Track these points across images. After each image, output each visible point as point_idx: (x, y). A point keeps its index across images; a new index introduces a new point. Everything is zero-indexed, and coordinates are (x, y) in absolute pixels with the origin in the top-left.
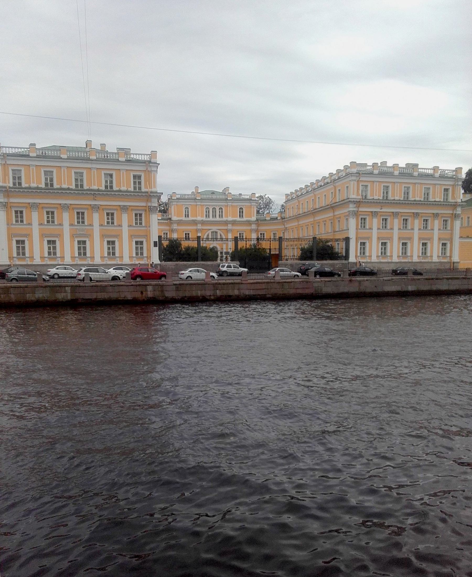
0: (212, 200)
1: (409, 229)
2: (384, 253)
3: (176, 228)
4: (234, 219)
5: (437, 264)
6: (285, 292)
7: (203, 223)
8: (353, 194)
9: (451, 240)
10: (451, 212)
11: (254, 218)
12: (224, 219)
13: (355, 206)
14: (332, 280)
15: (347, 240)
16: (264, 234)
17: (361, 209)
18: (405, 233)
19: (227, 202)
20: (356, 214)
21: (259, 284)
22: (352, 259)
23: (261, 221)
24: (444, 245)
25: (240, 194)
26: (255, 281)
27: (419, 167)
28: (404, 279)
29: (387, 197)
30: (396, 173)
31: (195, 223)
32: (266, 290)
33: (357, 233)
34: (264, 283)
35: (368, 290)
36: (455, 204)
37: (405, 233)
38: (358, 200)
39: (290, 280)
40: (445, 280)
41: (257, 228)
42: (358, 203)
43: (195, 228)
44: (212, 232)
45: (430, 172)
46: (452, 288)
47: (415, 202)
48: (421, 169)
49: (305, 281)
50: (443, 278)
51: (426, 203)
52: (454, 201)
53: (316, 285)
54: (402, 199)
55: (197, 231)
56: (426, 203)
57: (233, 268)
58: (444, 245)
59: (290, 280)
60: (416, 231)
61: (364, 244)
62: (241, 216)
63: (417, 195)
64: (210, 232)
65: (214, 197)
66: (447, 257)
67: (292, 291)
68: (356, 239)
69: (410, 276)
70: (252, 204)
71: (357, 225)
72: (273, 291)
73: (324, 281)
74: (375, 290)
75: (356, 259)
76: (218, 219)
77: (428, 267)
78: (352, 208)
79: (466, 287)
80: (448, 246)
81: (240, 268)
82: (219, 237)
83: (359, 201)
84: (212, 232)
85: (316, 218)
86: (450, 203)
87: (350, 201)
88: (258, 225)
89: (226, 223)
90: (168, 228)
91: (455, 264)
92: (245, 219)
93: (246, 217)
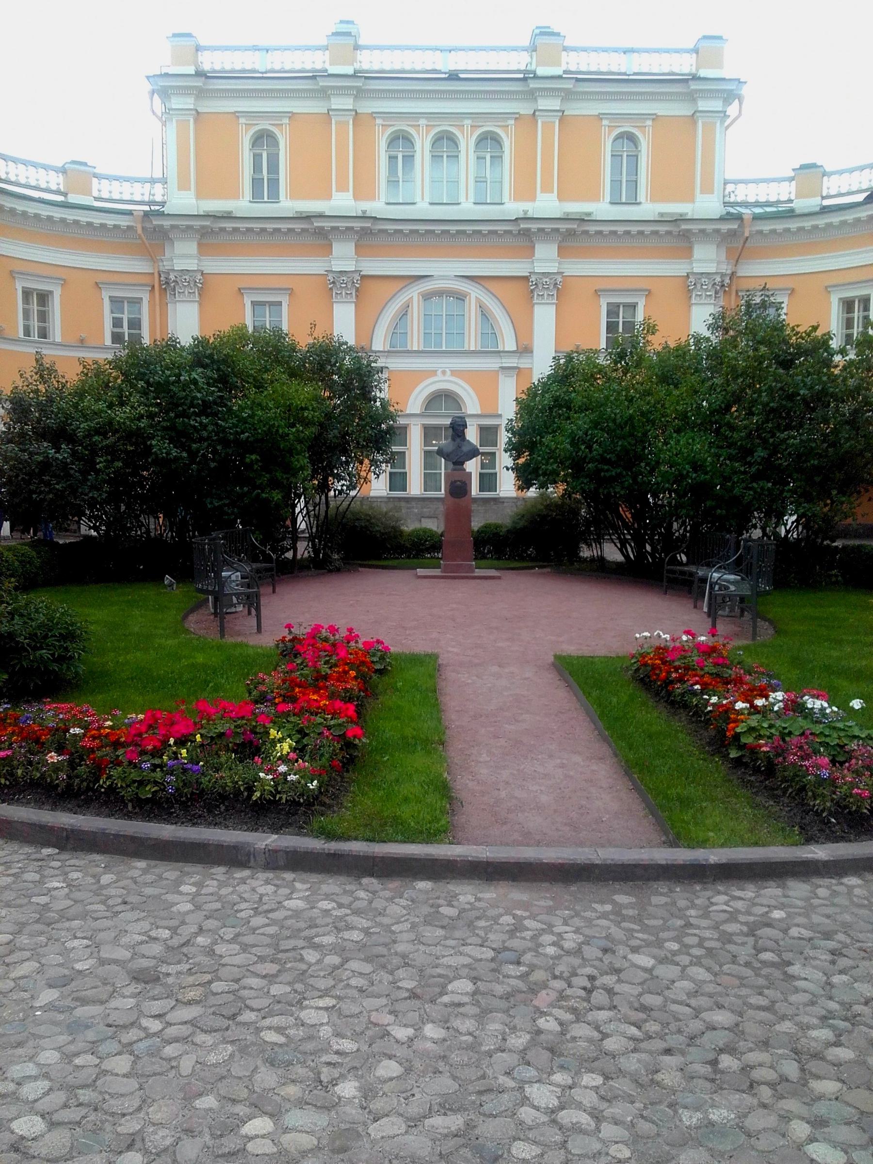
3: (191, 265)
4: (575, 208)
31: (315, 232)
41: (726, 269)
43: (314, 266)
44: (427, 296)
70: (702, 105)
84: (427, 296)
93: (654, 198)
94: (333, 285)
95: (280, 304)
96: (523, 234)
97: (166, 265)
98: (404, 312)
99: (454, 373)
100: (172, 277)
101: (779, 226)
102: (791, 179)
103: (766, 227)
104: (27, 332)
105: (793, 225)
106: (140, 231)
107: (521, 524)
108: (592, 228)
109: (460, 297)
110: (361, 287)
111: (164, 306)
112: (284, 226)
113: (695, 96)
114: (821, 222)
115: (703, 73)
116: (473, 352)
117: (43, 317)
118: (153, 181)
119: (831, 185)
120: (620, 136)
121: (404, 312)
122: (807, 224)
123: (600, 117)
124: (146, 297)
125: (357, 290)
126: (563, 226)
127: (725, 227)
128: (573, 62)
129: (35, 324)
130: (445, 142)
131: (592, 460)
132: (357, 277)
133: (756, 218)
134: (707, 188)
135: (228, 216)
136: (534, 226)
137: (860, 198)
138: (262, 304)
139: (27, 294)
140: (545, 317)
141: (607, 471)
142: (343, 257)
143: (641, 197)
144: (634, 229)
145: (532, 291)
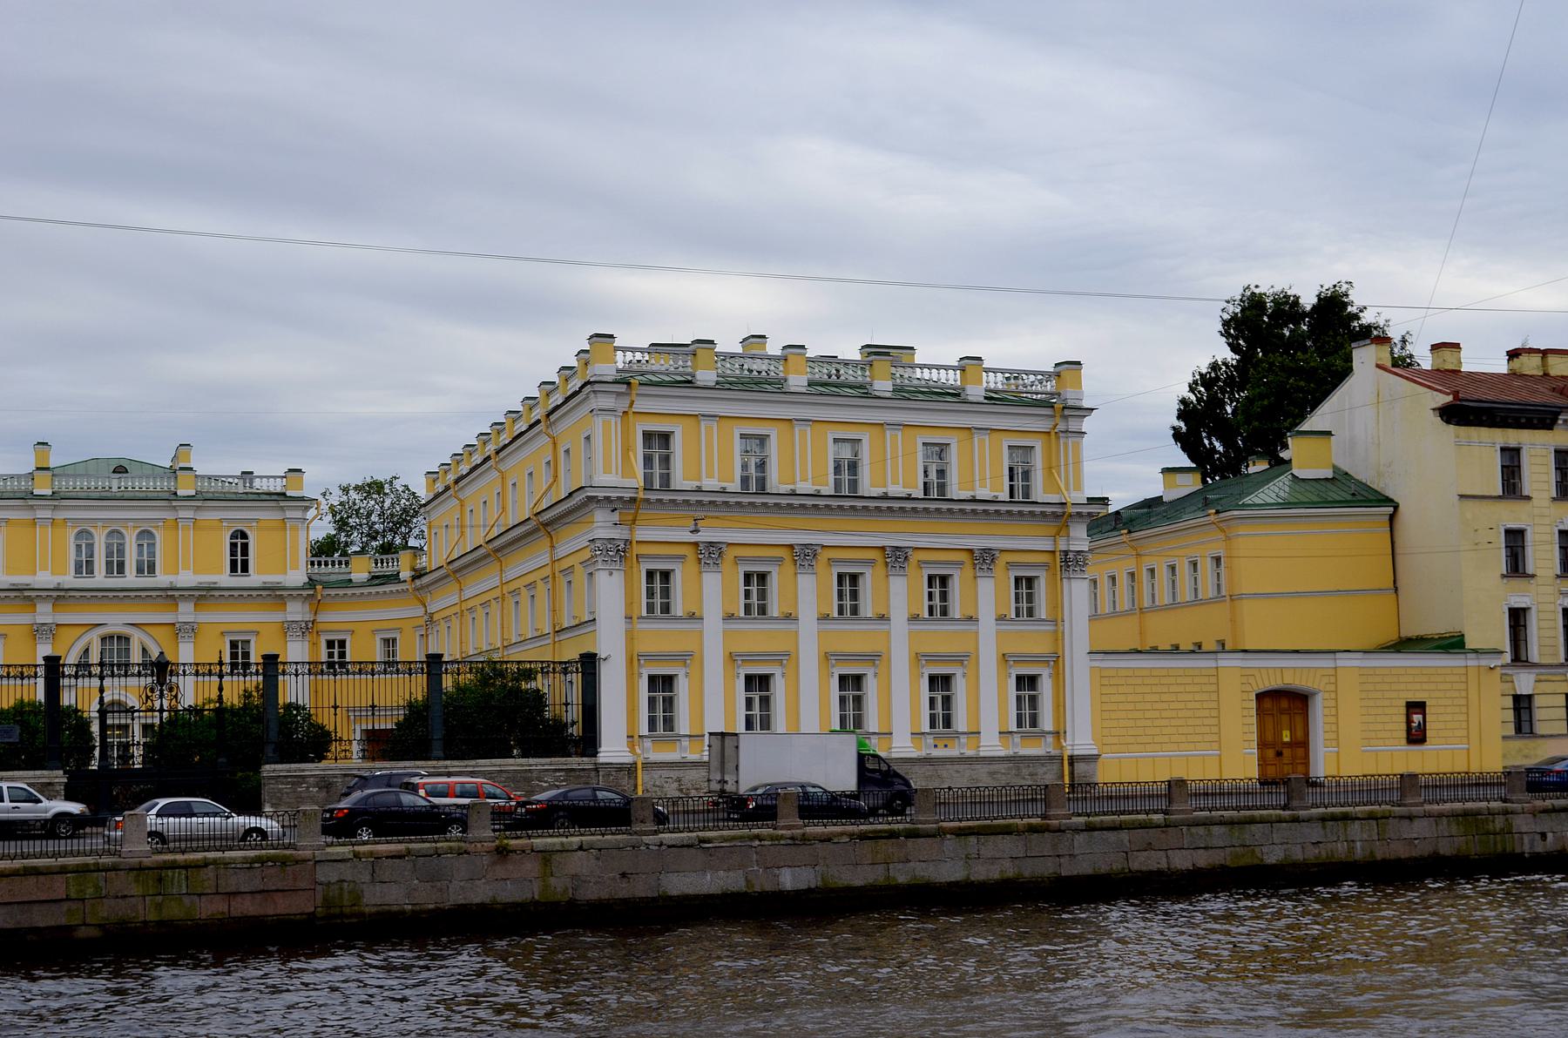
0: (105, 497)
1: (772, 618)
2: (943, 719)
5: (1002, 767)
6: (174, 911)
7: (60, 596)
8: (607, 471)
9: (1055, 660)
10: (1047, 545)
11: (296, 576)
12: (162, 579)
13: (616, 517)
14: (409, 852)
15: (589, 663)
16: (342, 644)
17: (642, 534)
18: (758, 637)
20: (620, 552)
21: (32, 880)
22: (613, 748)
23: (327, 585)
24: (1027, 682)
25: (247, 474)
26: (18, 864)
27: (918, 360)
28: (758, 837)
29: (762, 482)
30: (797, 381)
32: (74, 906)
33: (630, 637)
34: (63, 870)
35: (591, 893)
36: (1059, 510)
37: (852, 637)
38: (627, 495)
39: (200, 856)
40: (950, 843)
42: (627, 506)
43: (25, 619)
45: (952, 379)
46: (983, 872)
47: (884, 504)
48: (922, 367)
49: (269, 859)
50: (940, 833)
51: (847, 503)
52: (1055, 499)
53: (326, 874)
54: (829, 489)
55: (38, 632)
56: (847, 503)
57: (7, 804)
58: (1027, 682)
59: (200, 856)
60: (987, 625)
61: (667, 682)
62: (239, 564)
63: (983, 480)
64: (94, 638)
65: (126, 483)
66: (1044, 734)
67: (208, 908)
68: (630, 661)
69: (790, 823)
70: (289, 514)
71: (629, 604)
72: (107, 911)
73: (371, 854)
74: (624, 891)
75: (632, 750)
76: (131, 579)
77: (959, 779)
78: (602, 525)
79: (1045, 868)
80: (1046, 688)
81: (46, 803)
82: (136, 657)
83: (633, 500)
85: (511, 574)
86: (1038, 509)
87: (590, 499)
88: (317, 605)
89: (170, 596)
91: (1080, 768)
92: (255, 578)
109: (124, 639)
122: (358, 591)
123: (221, 520)
126: (197, 593)
127: (305, 593)
134: (295, 567)
136: (176, 594)
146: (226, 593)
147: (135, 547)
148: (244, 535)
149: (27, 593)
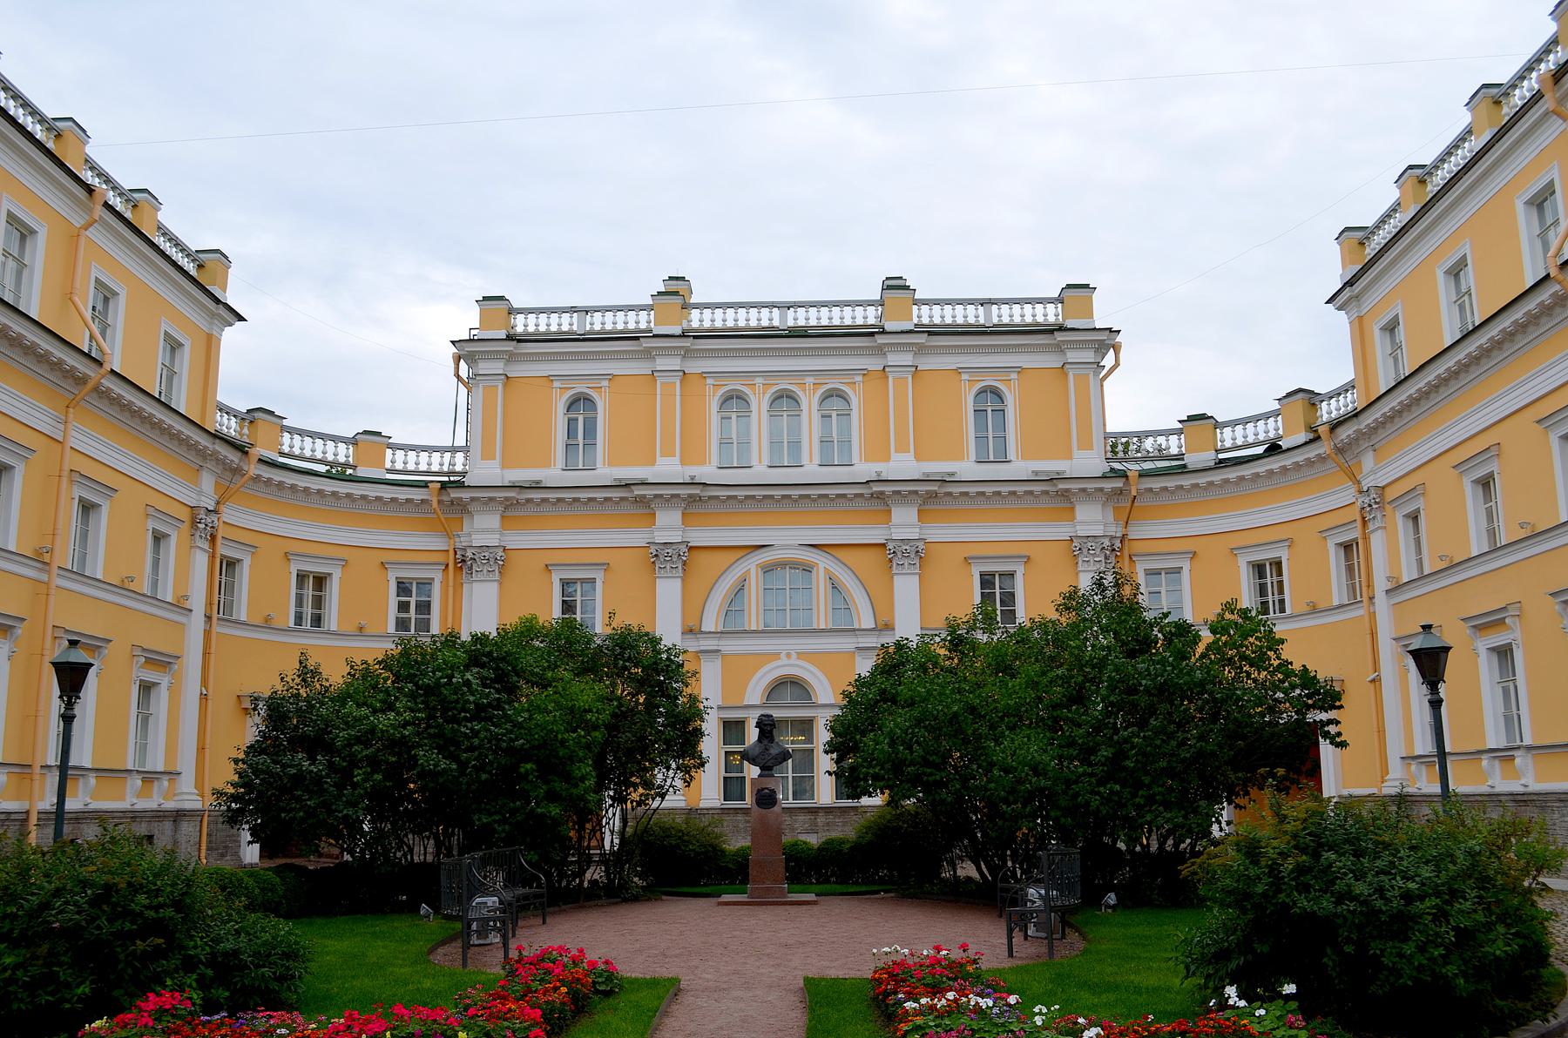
3: (492, 540)
19: (880, 351)
31: (635, 499)
43: (636, 537)
84: (768, 569)
90: (435, 543)
93: (1026, 455)
94: (657, 557)
95: (593, 581)
96: (878, 496)
97: (463, 542)
98: (740, 589)
99: (800, 655)
100: (469, 554)
101: (1171, 482)
102: (1179, 432)
103: (1156, 484)
104: (299, 619)
105: (1186, 481)
106: (435, 504)
107: (869, 837)
108: (956, 489)
109: (807, 569)
110: (685, 558)
111: (458, 587)
112: (600, 495)
113: (1071, 338)
114: (1217, 477)
115: (1070, 324)
116: (823, 631)
117: (318, 602)
118: (454, 450)
119: (1227, 437)
120: (982, 391)
121: (740, 589)
122: (1202, 480)
123: (958, 371)
124: (438, 576)
125: (684, 563)
127: (1108, 485)
128: (925, 315)
129: (308, 610)
130: (785, 398)
131: (912, 763)
132: (683, 548)
133: (1143, 474)
134: (1086, 444)
135: (537, 486)
136: (888, 489)
137: (1260, 450)
138: (574, 581)
139: (302, 577)
140: (906, 588)
141: (931, 774)
142: (669, 526)
143: (1011, 455)
144: (1005, 489)
145: (891, 560)
146: (972, 489)
147: (816, 416)
148: (997, 394)
149: (638, 491)
